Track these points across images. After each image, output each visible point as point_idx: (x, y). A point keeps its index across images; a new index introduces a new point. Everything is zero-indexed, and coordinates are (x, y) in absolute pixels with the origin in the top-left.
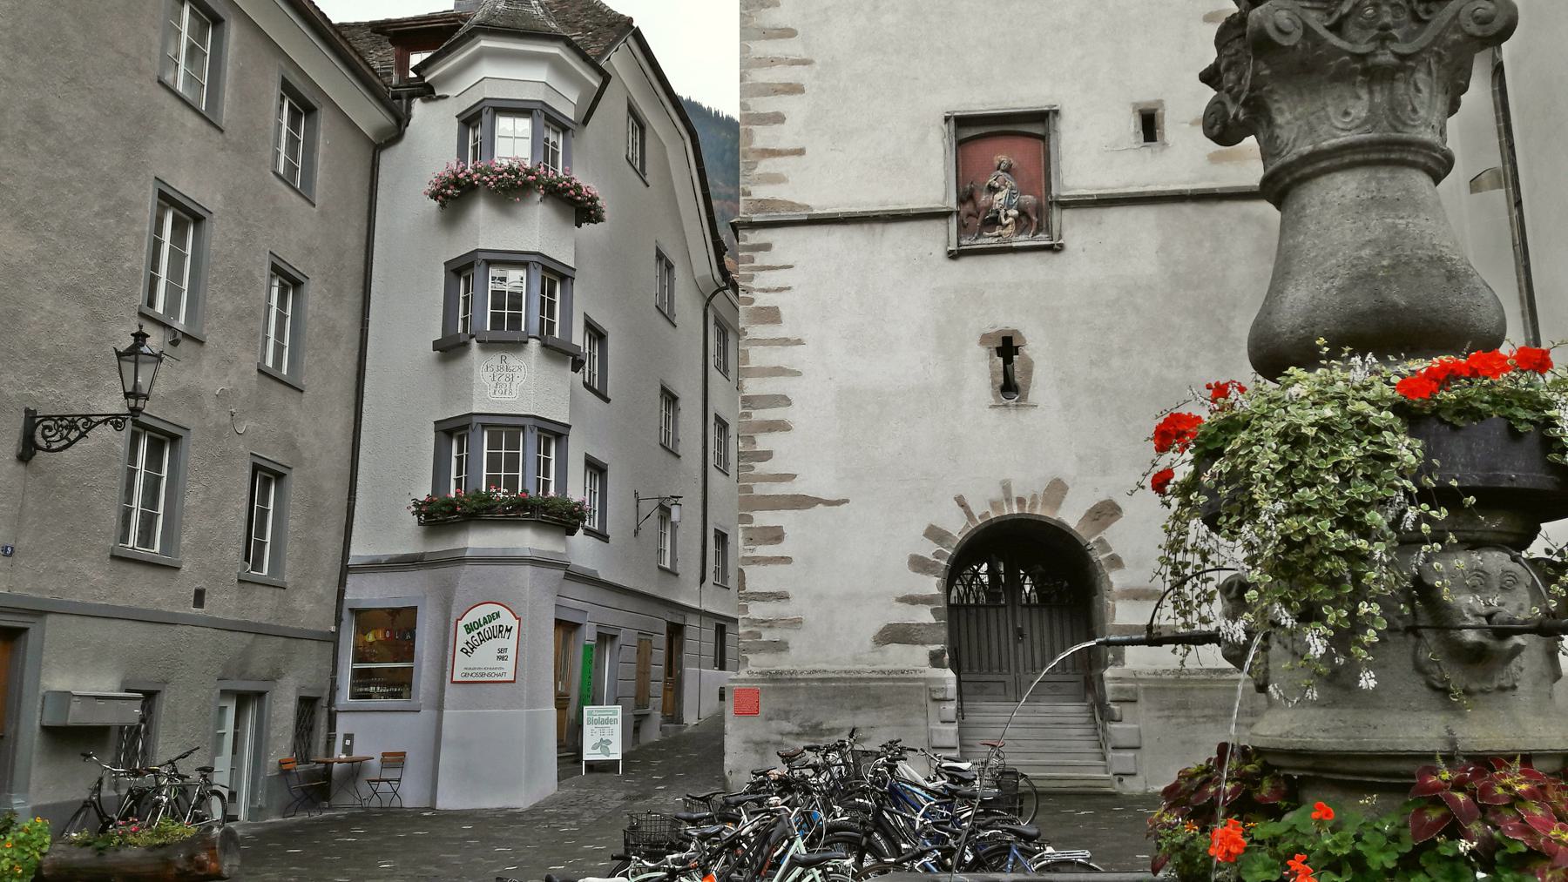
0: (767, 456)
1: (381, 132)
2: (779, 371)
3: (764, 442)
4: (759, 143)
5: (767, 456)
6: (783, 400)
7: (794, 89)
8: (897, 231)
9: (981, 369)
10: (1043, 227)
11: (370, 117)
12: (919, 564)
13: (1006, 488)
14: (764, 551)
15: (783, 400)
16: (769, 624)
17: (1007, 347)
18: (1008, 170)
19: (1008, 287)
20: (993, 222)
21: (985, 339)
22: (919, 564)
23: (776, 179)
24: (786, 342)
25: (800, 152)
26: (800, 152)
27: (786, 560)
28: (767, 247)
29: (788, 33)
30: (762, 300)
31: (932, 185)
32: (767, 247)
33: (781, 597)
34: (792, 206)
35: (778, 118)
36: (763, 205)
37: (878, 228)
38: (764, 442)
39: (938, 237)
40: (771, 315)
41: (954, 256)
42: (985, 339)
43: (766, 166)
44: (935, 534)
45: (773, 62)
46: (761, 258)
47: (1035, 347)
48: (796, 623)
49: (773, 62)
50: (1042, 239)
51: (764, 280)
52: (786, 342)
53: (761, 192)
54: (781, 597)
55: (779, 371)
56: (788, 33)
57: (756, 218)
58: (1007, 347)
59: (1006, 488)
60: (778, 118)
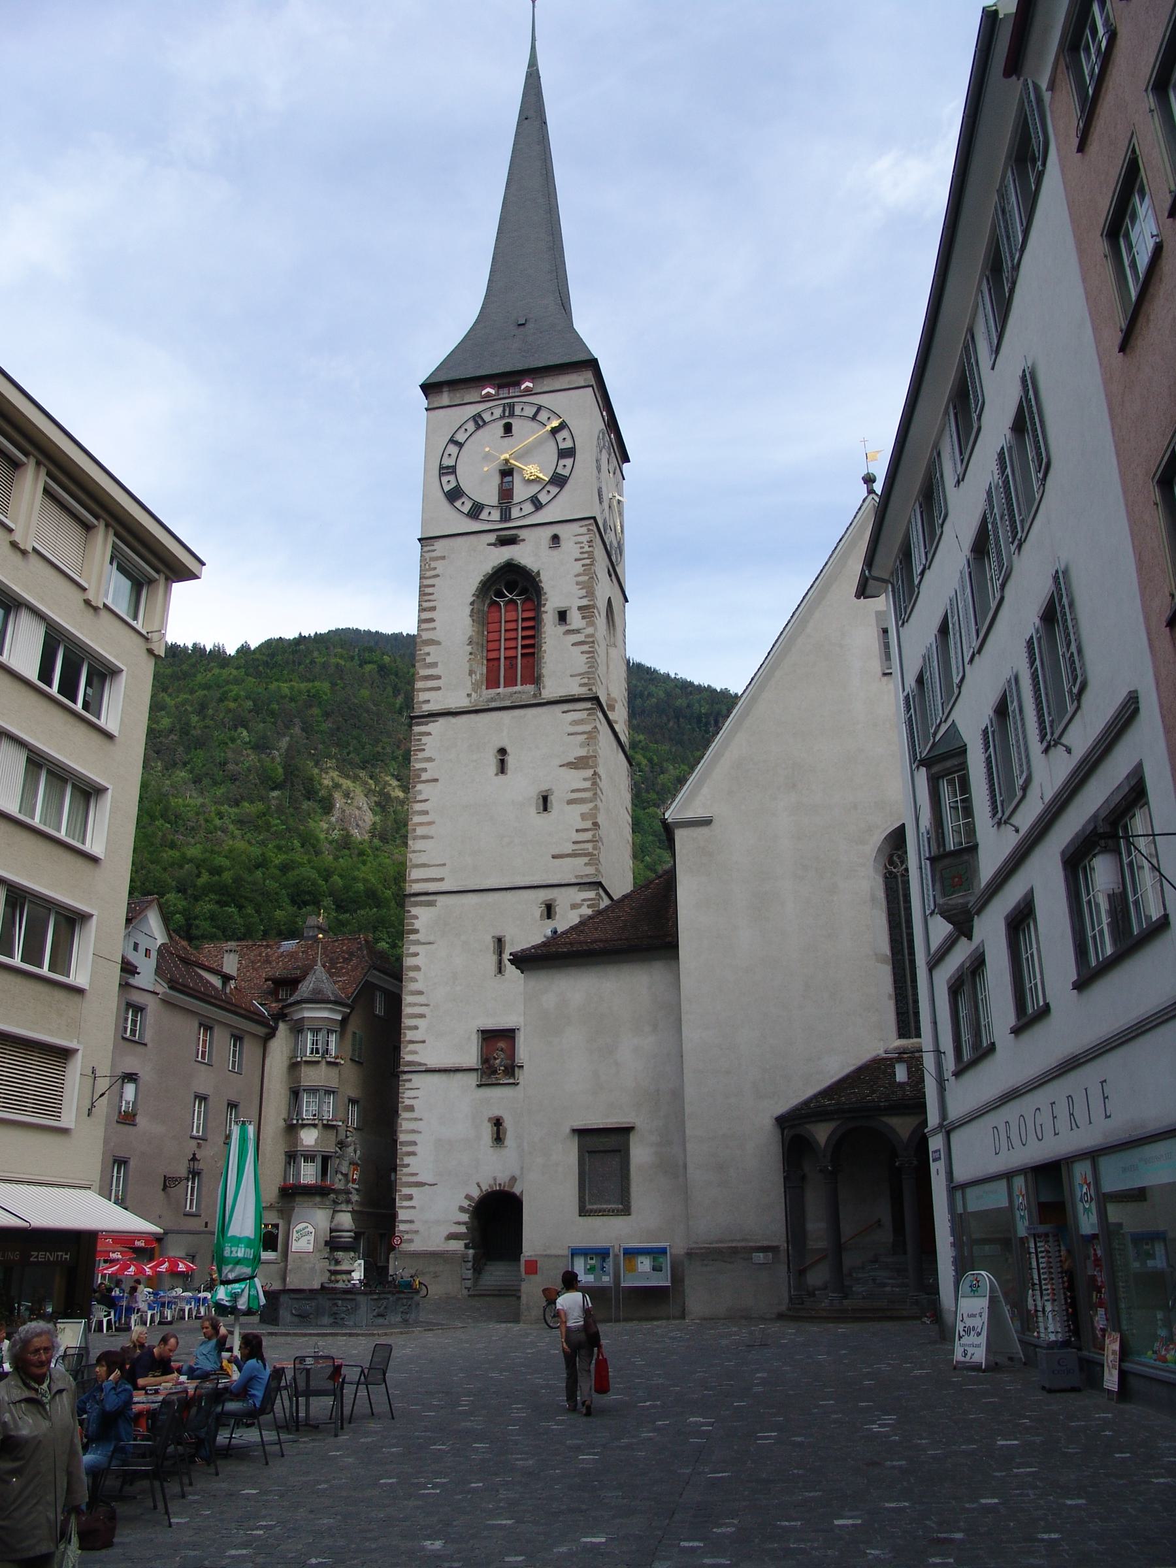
0: (408, 1165)
1: (267, 1034)
2: (413, 1131)
3: (407, 1160)
4: (408, 1038)
5: (408, 1165)
6: (415, 1143)
7: (422, 1016)
8: (459, 1076)
9: (487, 1131)
10: (513, 1075)
11: (261, 1031)
12: (462, 1209)
13: (495, 1179)
14: (405, 1204)
15: (415, 1143)
16: (407, 1232)
17: (498, 1123)
18: (502, 1050)
19: (499, 1099)
20: (495, 1072)
21: (490, 1120)
22: (462, 1209)
23: (415, 1053)
24: (416, 1119)
25: (424, 1042)
26: (424, 1042)
27: (414, 1207)
28: (410, 1080)
29: (421, 993)
30: (408, 1102)
31: (471, 1056)
32: (410, 1080)
33: (411, 1222)
34: (420, 1064)
35: (416, 1028)
36: (410, 1063)
37: (452, 1074)
38: (407, 1160)
39: (472, 1079)
40: (411, 1108)
41: (479, 1086)
42: (490, 1120)
43: (411, 1047)
44: (468, 1197)
45: (415, 1005)
46: (408, 1085)
47: (508, 1124)
48: (417, 1232)
49: (415, 1005)
50: (511, 1081)
51: (409, 1094)
52: (416, 1119)
53: (408, 1058)
54: (411, 1222)
55: (413, 1131)
56: (421, 993)
57: (406, 1069)
58: (498, 1123)
59: (495, 1179)
60: (416, 1028)
